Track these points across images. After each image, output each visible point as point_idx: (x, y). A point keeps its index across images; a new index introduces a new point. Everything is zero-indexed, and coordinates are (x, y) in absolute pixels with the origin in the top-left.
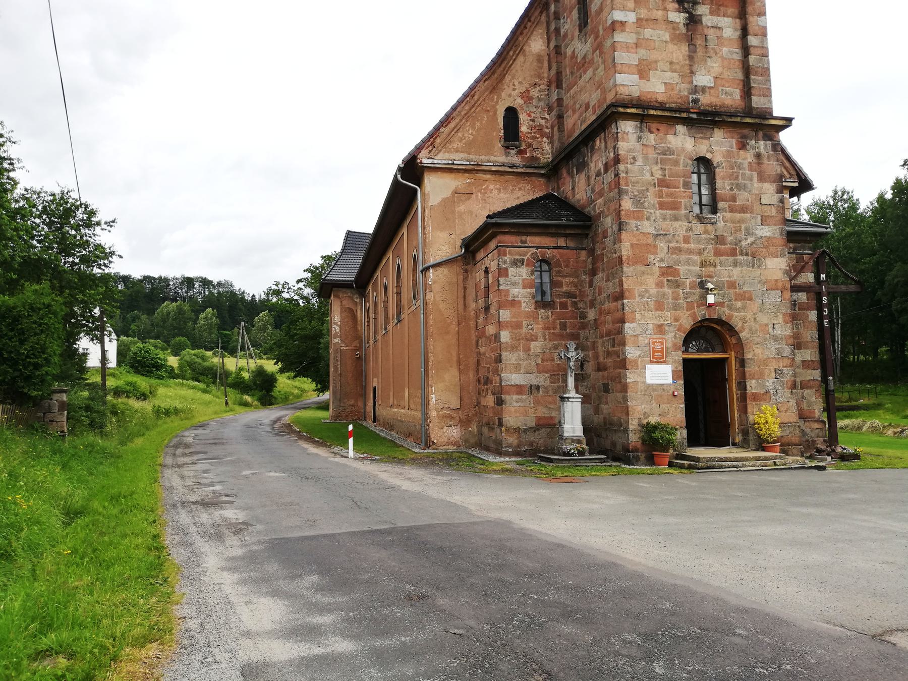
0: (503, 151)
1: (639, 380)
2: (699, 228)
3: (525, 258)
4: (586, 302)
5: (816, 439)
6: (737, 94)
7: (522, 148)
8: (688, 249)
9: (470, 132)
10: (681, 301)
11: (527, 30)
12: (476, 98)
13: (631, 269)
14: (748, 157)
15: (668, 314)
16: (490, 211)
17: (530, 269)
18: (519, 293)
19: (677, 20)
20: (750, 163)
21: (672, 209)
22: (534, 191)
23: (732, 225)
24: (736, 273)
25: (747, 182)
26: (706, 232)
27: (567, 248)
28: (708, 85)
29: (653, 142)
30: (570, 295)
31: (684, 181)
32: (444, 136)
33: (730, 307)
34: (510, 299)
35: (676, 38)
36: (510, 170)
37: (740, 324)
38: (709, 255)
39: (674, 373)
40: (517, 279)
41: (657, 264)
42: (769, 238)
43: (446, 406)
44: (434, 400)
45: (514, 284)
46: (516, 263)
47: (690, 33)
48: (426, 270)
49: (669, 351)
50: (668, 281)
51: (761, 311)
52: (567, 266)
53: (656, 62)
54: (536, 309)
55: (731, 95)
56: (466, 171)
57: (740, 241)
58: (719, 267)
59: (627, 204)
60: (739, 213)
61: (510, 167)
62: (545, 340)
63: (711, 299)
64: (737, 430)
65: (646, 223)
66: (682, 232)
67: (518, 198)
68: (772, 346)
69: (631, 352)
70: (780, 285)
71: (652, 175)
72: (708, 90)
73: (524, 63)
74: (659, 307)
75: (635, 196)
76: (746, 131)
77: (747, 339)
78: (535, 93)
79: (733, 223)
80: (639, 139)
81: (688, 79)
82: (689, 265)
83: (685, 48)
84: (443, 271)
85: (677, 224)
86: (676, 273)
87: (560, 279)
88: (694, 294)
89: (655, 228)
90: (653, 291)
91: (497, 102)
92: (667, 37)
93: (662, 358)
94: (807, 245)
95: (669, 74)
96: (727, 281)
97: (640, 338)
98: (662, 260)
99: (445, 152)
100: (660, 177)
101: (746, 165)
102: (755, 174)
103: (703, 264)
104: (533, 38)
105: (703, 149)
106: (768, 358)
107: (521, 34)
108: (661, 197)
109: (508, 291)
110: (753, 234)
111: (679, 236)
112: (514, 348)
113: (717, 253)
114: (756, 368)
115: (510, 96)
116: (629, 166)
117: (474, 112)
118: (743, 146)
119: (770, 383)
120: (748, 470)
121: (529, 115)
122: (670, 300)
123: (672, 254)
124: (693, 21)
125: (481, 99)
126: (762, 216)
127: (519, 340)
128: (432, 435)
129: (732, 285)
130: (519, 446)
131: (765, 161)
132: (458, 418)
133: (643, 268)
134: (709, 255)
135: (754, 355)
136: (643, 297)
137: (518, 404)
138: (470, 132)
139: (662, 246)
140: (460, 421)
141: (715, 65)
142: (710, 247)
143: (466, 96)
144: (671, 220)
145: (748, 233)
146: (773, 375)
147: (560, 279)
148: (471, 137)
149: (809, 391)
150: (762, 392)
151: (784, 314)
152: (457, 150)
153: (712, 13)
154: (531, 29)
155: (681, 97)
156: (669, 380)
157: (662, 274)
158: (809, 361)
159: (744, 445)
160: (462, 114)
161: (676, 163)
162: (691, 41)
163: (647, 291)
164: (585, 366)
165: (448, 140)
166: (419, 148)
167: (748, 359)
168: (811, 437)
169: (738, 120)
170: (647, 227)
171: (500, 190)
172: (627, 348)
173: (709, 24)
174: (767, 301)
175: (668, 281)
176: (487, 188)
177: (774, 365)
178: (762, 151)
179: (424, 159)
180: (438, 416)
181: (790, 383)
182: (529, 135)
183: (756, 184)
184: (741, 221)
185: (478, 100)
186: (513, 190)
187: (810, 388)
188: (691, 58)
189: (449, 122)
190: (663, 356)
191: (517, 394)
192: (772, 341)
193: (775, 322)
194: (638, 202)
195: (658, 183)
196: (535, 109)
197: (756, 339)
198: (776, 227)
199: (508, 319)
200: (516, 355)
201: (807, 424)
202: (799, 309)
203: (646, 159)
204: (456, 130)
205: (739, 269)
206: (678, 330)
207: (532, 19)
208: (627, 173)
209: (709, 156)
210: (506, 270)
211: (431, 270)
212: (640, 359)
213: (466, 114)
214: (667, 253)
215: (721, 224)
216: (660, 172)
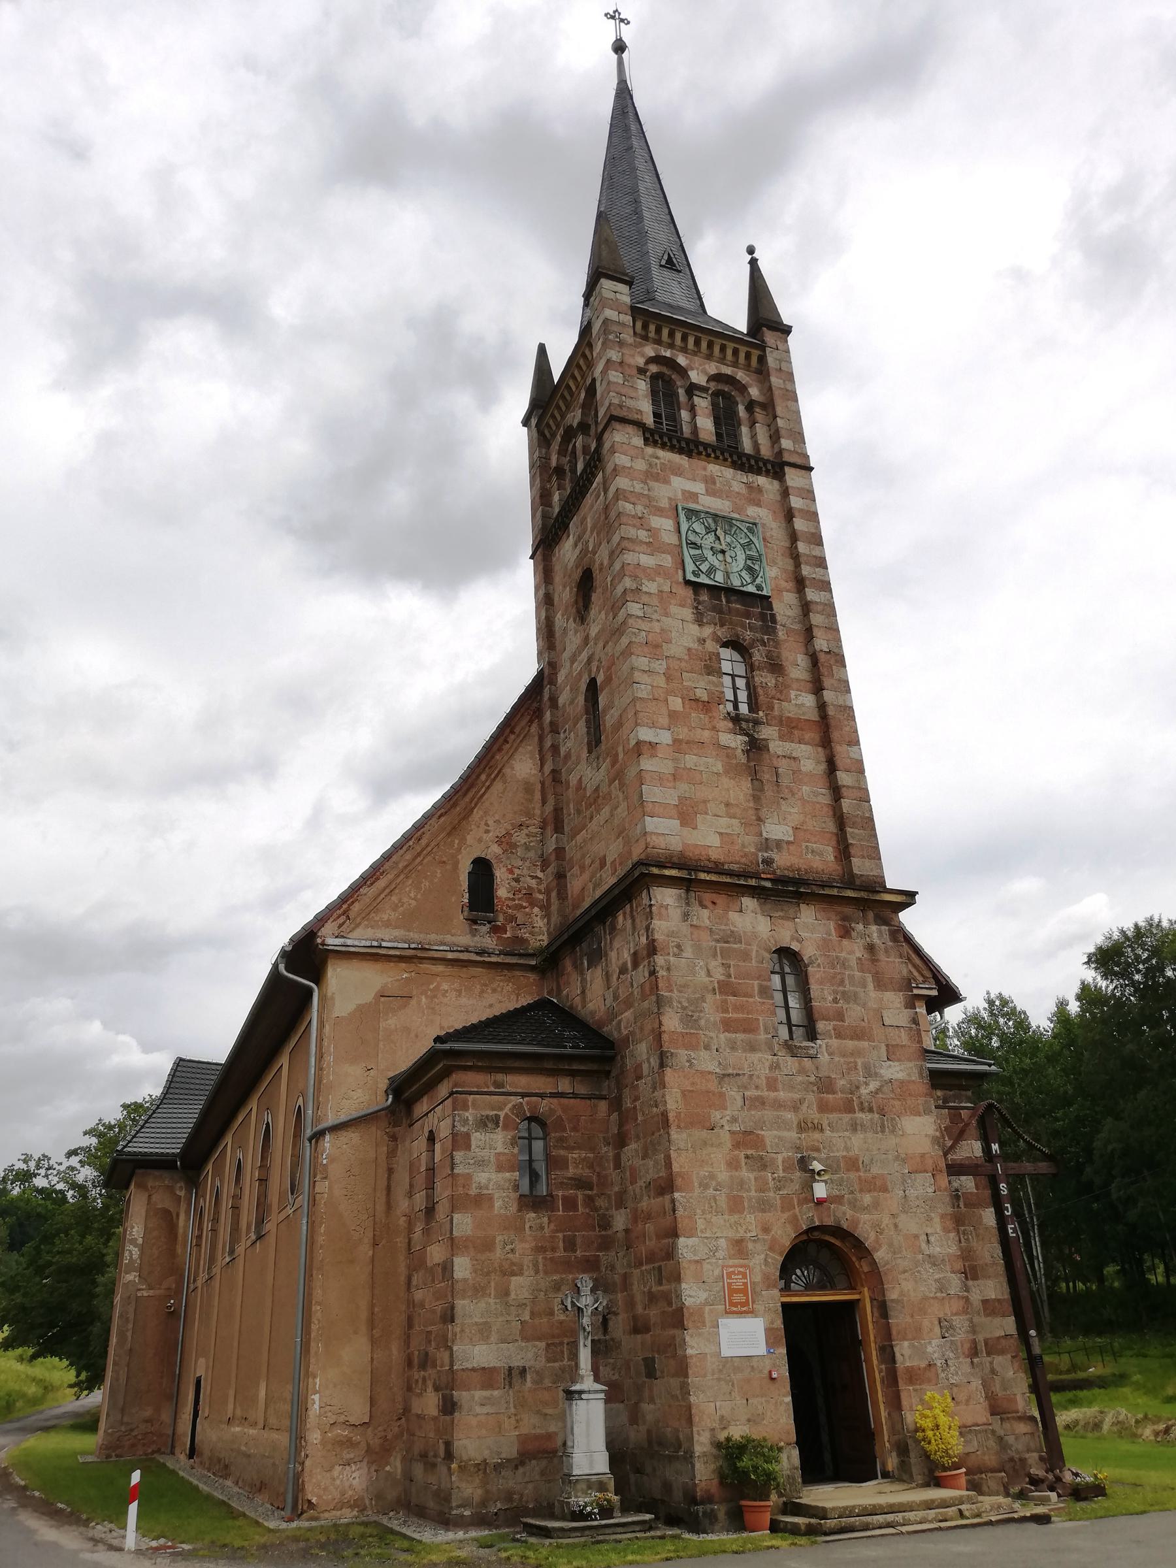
0: (467, 929)
1: (709, 1349)
2: (790, 1064)
3: (502, 1114)
4: (609, 1197)
5: (1027, 1456)
6: (829, 853)
7: (499, 923)
8: (775, 1100)
9: (412, 895)
10: (771, 1194)
11: (508, 746)
12: (424, 842)
13: (684, 1136)
14: (854, 950)
15: (751, 1218)
16: (442, 1028)
17: (510, 1135)
18: (489, 1180)
19: (733, 745)
20: (859, 959)
21: (745, 1031)
22: (518, 995)
23: (842, 1060)
24: (858, 1143)
25: (858, 989)
26: (802, 1071)
27: (575, 1096)
28: (786, 838)
29: (707, 922)
30: (581, 1183)
31: (760, 986)
32: (366, 900)
33: (853, 1205)
34: (473, 1192)
35: (732, 770)
36: (479, 958)
37: (872, 1236)
39: (768, 1331)
40: (485, 1153)
41: (727, 1128)
42: (902, 1082)
43: (342, 1419)
44: (316, 1406)
45: (481, 1164)
46: (485, 1123)
47: (752, 764)
48: (318, 1136)
49: (758, 1289)
50: (747, 1157)
52: (575, 1129)
53: (705, 802)
54: (520, 1210)
55: (821, 854)
56: (401, 959)
57: (858, 1088)
58: (828, 1133)
59: (671, 1022)
60: (852, 1039)
61: (477, 954)
62: (537, 1272)
63: (820, 1190)
64: (887, 1444)
65: (703, 1054)
66: (764, 1071)
67: (491, 1006)
68: (931, 1275)
69: (692, 1294)
70: (929, 1163)
71: (709, 974)
72: (785, 846)
73: (503, 793)
74: (736, 1205)
75: (684, 1008)
76: (848, 910)
77: (887, 1263)
78: (520, 838)
79: (844, 1056)
80: (686, 916)
82: (779, 1128)
83: (746, 785)
84: (352, 1137)
85: (755, 1057)
86: (759, 1143)
87: (562, 1152)
88: (792, 1181)
89: (720, 1064)
90: (723, 1175)
91: (459, 850)
92: (719, 767)
93: (746, 1304)
94: (964, 1093)
95: (724, 821)
96: (843, 1157)
97: (706, 1266)
98: (734, 1120)
99: (367, 927)
100: (722, 978)
101: (853, 963)
103: (803, 1127)
104: (517, 756)
105: (785, 937)
106: (925, 1298)
107: (500, 750)
108: (726, 1011)
109: (469, 1177)
110: (876, 1074)
111: (758, 1077)
112: (478, 1291)
113: (823, 1108)
114: (908, 1319)
115: (480, 840)
116: (672, 959)
117: (421, 863)
118: (845, 933)
119: (934, 1347)
121: (511, 872)
122: (753, 1193)
123: (749, 1109)
124: (755, 747)
125: (433, 844)
126: (887, 1046)
127: (488, 1274)
128: (309, 1487)
129: (853, 1164)
130: (484, 1503)
131: (882, 956)
132: (363, 1445)
133: (705, 1134)
134: (814, 1115)
135: (902, 1294)
136: (706, 1187)
137: (485, 1410)
138: (412, 895)
139: (733, 1094)
140: (369, 1450)
141: (793, 812)
142: (811, 1097)
143: (407, 838)
144: (745, 1051)
145: (870, 1073)
146: (937, 1330)
147: (562, 1152)
148: (414, 903)
150: (923, 1364)
151: (942, 1216)
152: (388, 924)
153: (782, 738)
154: (515, 745)
155: (746, 855)
156: (762, 1349)
157: (737, 1145)
159: (902, 1476)
160: (401, 866)
161: (746, 956)
163: (712, 1176)
164: (611, 1324)
165: (374, 907)
166: (321, 919)
167: (893, 1301)
168: (1017, 1451)
169: (835, 892)
170: (707, 1062)
171: (460, 991)
172: (684, 1286)
173: (780, 753)
174: (911, 1193)
175: (747, 1157)
176: (437, 988)
177: (936, 1310)
178: (876, 939)
179: (330, 938)
180: (323, 1442)
181: (967, 1346)
182: (510, 903)
183: (872, 995)
184: (857, 1053)
185: (427, 846)
186: (482, 992)
187: (1002, 1352)
188: (756, 799)
189: (378, 879)
190: (747, 1300)
191: (483, 1388)
192: (928, 1266)
193: (929, 1231)
194: (689, 1019)
195: (719, 988)
196: (520, 863)
198: (911, 1064)
199: (469, 1232)
200: (482, 1305)
201: (1007, 1425)
202: (966, 1206)
203: (698, 948)
204: (387, 891)
205: (860, 1135)
206: (771, 1249)
207: (517, 730)
208: (668, 969)
209: (795, 946)
210: (467, 1136)
211: (327, 1137)
212: (707, 1308)
213: (407, 866)
214: (742, 1107)
215: (824, 1058)
216: (721, 970)
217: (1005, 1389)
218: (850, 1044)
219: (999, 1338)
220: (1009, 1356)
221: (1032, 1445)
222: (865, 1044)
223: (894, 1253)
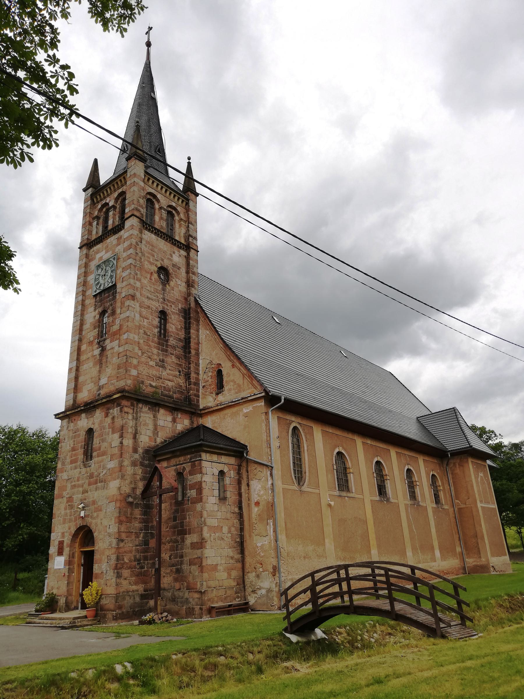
5: (195, 607)
14: (109, 420)
21: (75, 463)
38: (86, 486)
39: (65, 561)
42: (112, 468)
51: (105, 518)
58: (89, 493)
81: (97, 384)
101: (107, 427)
102: (111, 430)
103: (83, 493)
106: (105, 549)
114: (99, 556)
120: (39, 626)
134: (86, 486)
146: (106, 560)
149: (194, 566)
156: (62, 567)
158: (195, 543)
162: (101, 364)
168: (193, 605)
177: (107, 553)
178: (115, 414)
181: (114, 566)
184: (102, 461)
187: (195, 564)
188: (100, 371)
192: (108, 537)
194: (63, 464)
197: (101, 537)
201: (191, 594)
217: (193, 580)
218: (100, 458)
219: (194, 558)
220: (197, 566)
221: (199, 603)
222: (105, 457)
223: (99, 533)
